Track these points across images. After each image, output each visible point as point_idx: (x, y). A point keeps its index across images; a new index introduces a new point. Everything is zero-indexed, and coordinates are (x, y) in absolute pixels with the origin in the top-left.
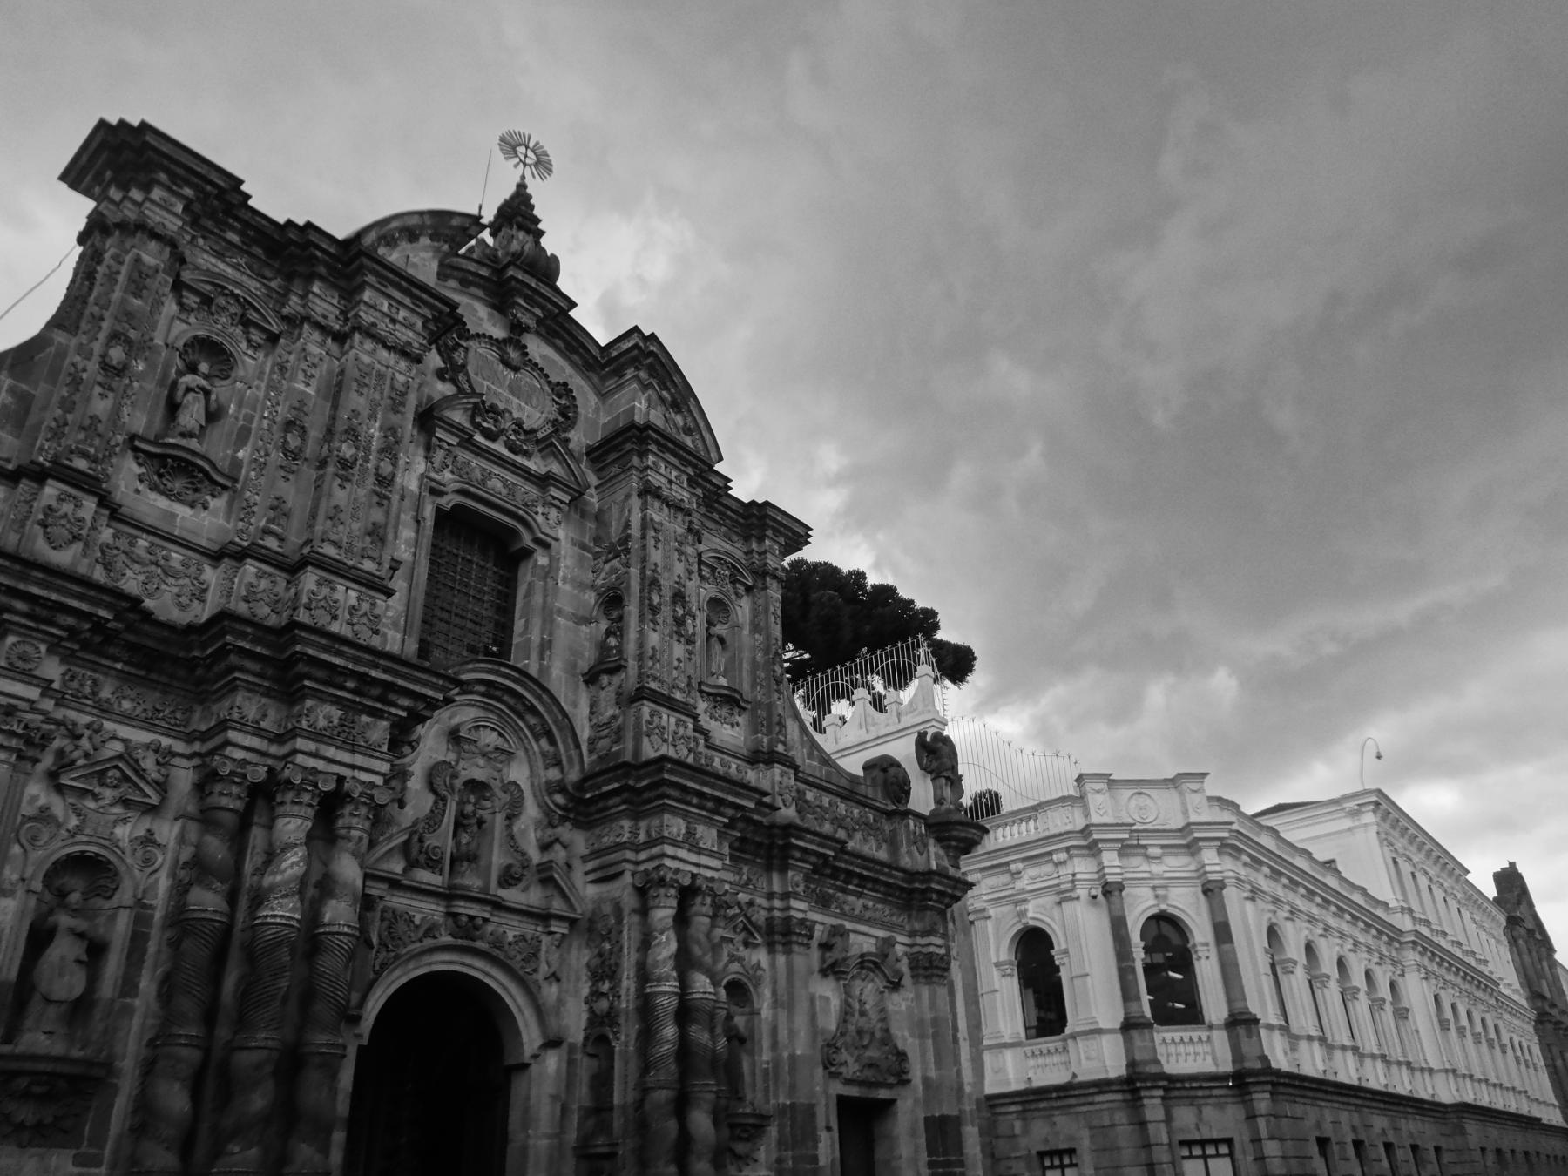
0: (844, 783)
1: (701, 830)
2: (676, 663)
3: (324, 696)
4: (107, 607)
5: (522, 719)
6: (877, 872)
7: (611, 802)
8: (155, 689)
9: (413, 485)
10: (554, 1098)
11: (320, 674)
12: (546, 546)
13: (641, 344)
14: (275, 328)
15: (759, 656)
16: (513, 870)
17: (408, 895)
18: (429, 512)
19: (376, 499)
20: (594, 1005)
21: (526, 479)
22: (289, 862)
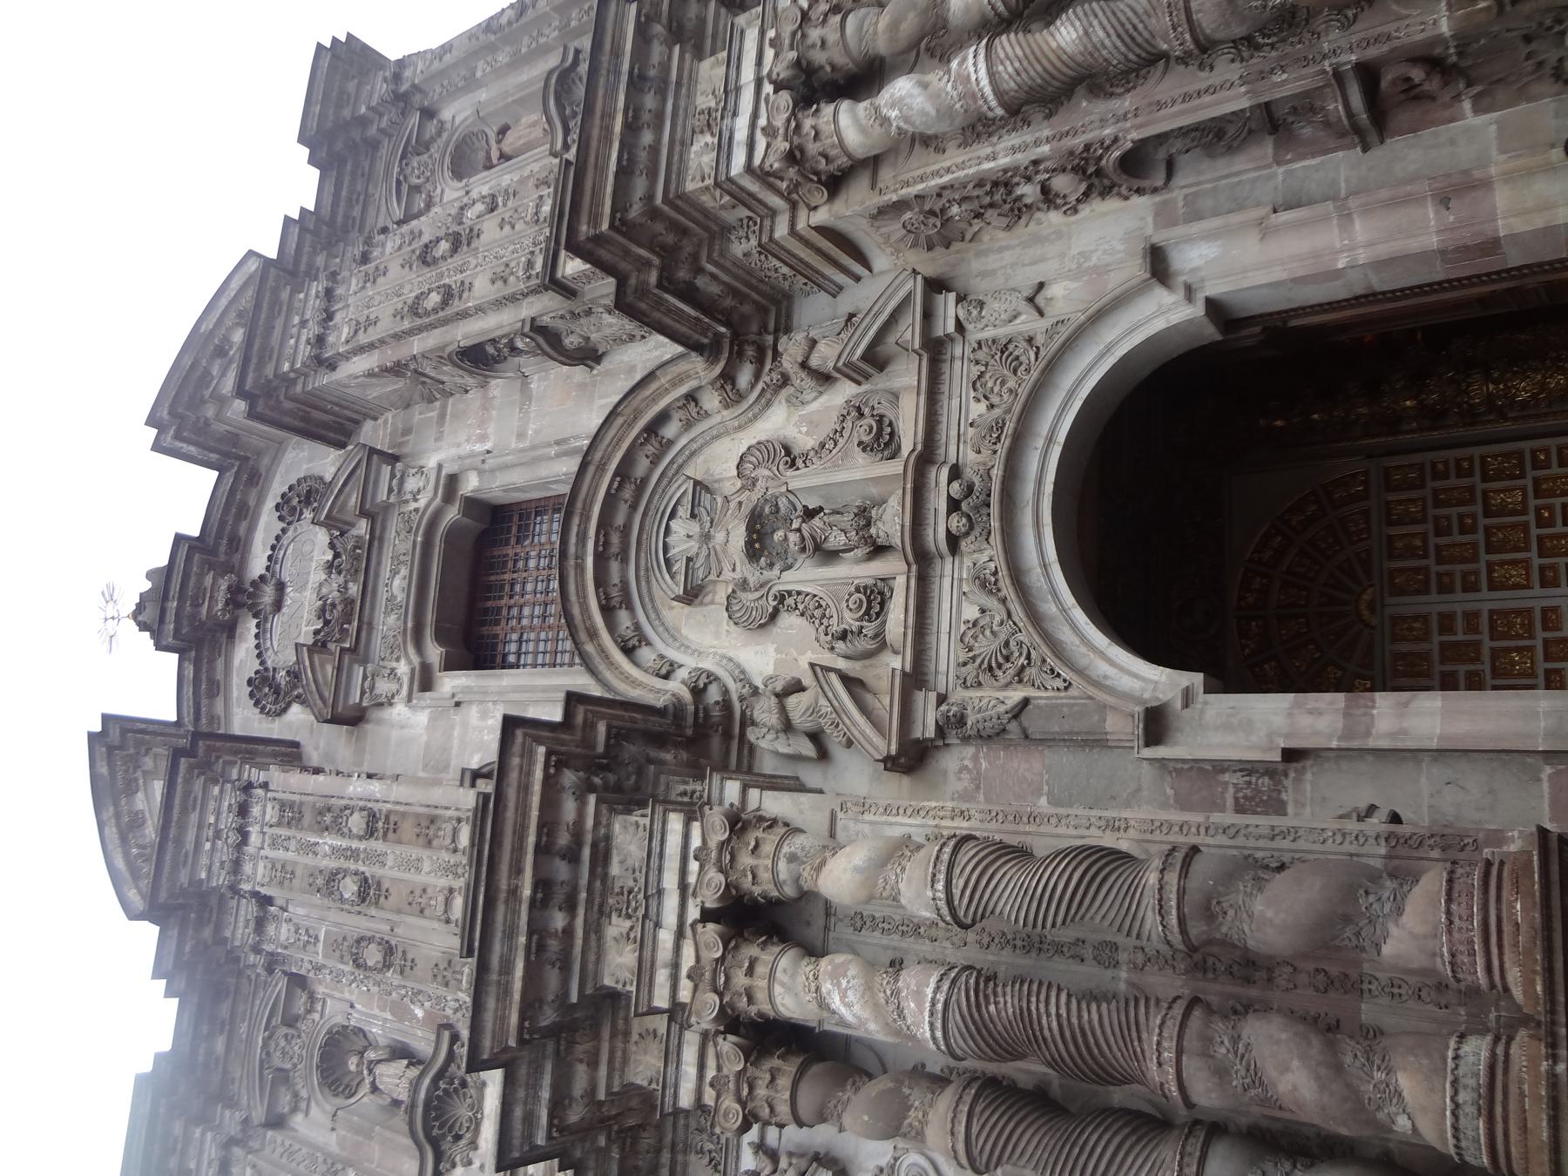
1: (704, 101)
2: (507, 228)
3: (592, 958)
5: (644, 481)
7: (715, 289)
8: (686, 1165)
9: (422, 718)
10: (1265, 230)
11: (553, 978)
12: (453, 481)
13: (172, 432)
14: (282, 984)
15: (503, 58)
16: (866, 439)
17: (933, 639)
18: (451, 683)
19: (391, 835)
20: (1072, 199)
21: (381, 540)
22: (843, 1010)
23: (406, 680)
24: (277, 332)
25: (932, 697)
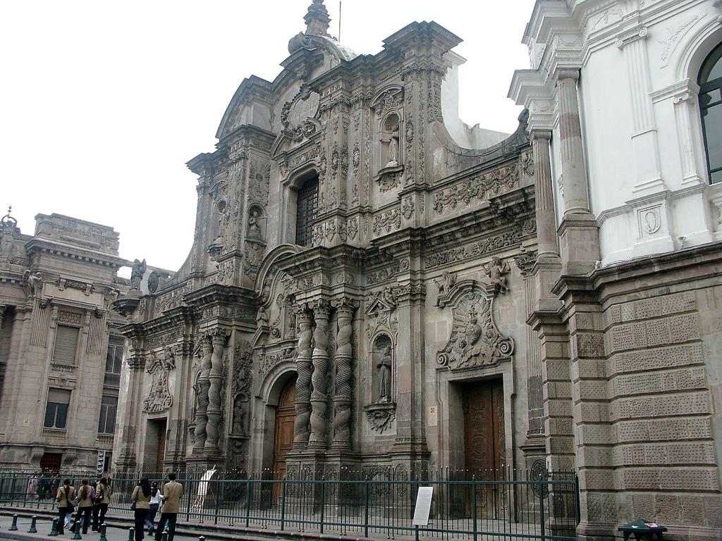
4: (179, 312)
17: (272, 349)
18: (287, 192)
23: (285, 178)
24: (329, 83)
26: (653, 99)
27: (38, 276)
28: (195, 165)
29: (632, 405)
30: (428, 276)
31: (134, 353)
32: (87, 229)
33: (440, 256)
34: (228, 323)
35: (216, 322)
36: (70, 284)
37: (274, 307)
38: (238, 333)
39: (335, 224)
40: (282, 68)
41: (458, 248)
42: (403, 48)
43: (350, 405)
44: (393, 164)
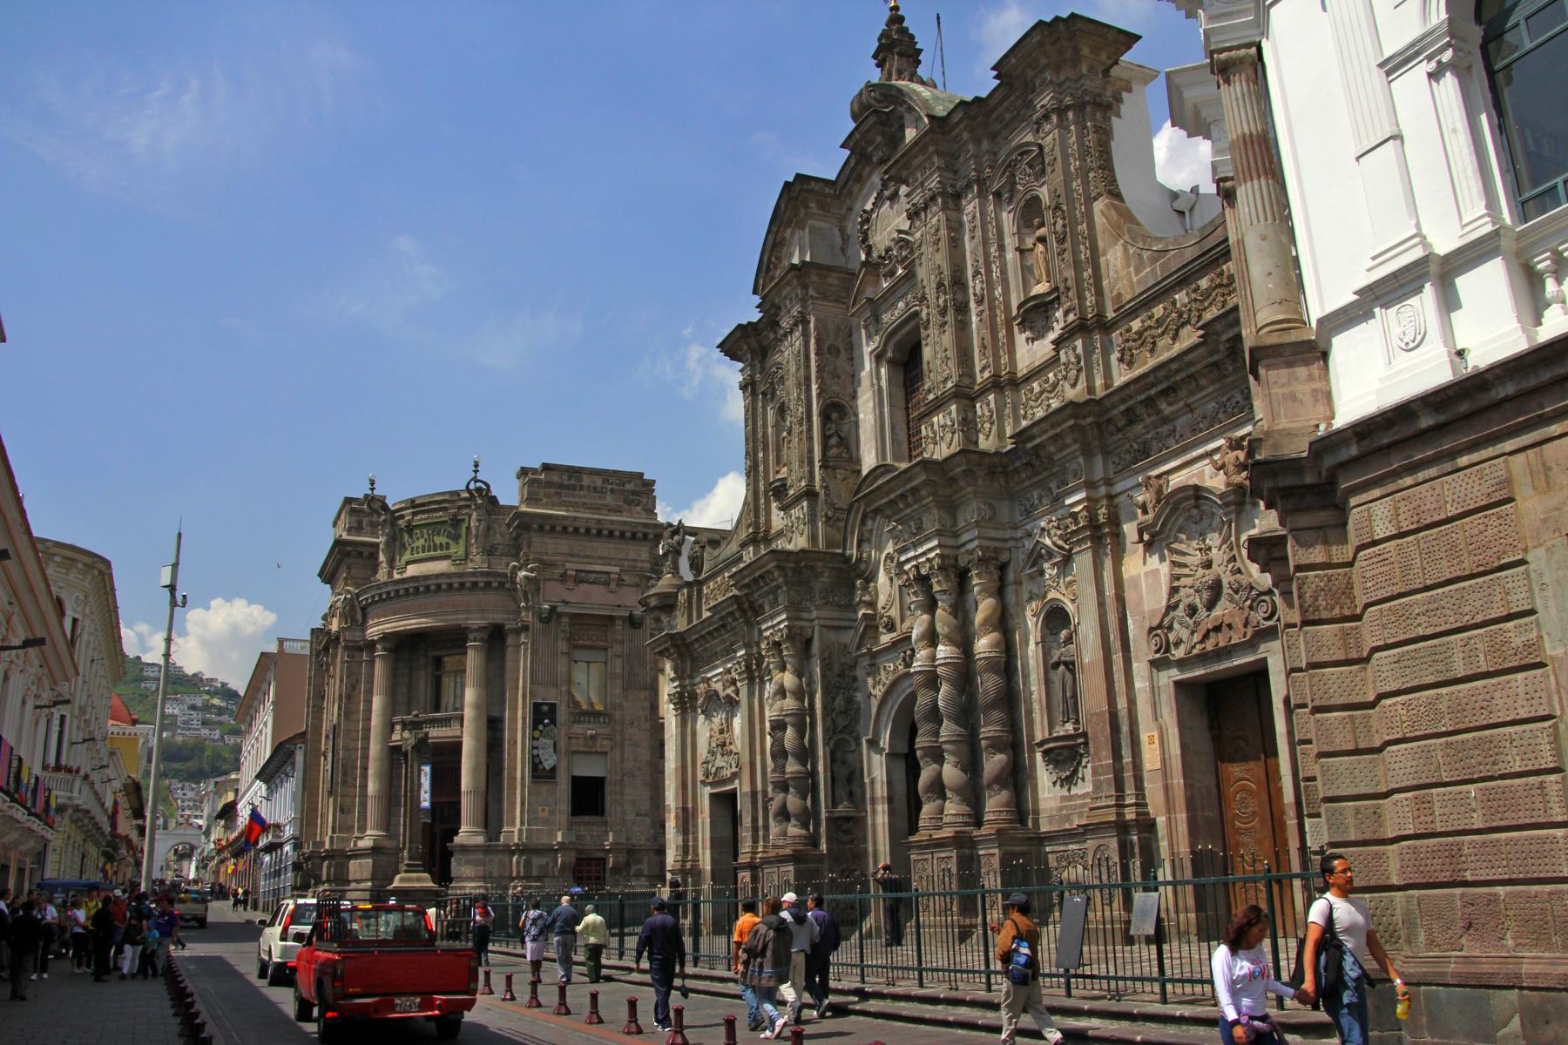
0: (1190, 254)
4: (732, 605)
6: (1167, 377)
24: (916, 162)
25: (868, 662)
26: (1388, 74)
27: (532, 570)
28: (730, 348)
29: (1404, 712)
30: (1119, 487)
31: (676, 683)
32: (599, 482)
33: (1135, 446)
34: (805, 615)
35: (784, 616)
36: (580, 578)
37: (882, 578)
38: (824, 630)
39: (954, 414)
40: (848, 152)
41: (1166, 427)
42: (1030, 73)
43: (1013, 744)
44: (1041, 288)
